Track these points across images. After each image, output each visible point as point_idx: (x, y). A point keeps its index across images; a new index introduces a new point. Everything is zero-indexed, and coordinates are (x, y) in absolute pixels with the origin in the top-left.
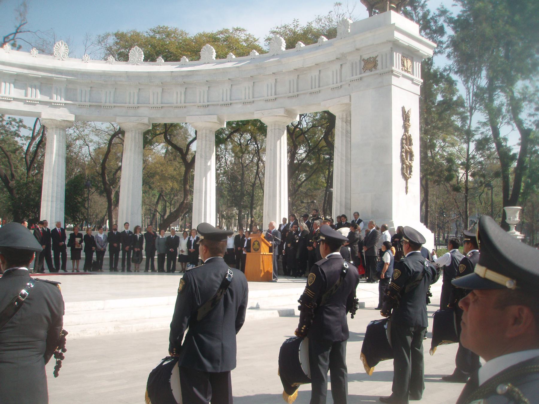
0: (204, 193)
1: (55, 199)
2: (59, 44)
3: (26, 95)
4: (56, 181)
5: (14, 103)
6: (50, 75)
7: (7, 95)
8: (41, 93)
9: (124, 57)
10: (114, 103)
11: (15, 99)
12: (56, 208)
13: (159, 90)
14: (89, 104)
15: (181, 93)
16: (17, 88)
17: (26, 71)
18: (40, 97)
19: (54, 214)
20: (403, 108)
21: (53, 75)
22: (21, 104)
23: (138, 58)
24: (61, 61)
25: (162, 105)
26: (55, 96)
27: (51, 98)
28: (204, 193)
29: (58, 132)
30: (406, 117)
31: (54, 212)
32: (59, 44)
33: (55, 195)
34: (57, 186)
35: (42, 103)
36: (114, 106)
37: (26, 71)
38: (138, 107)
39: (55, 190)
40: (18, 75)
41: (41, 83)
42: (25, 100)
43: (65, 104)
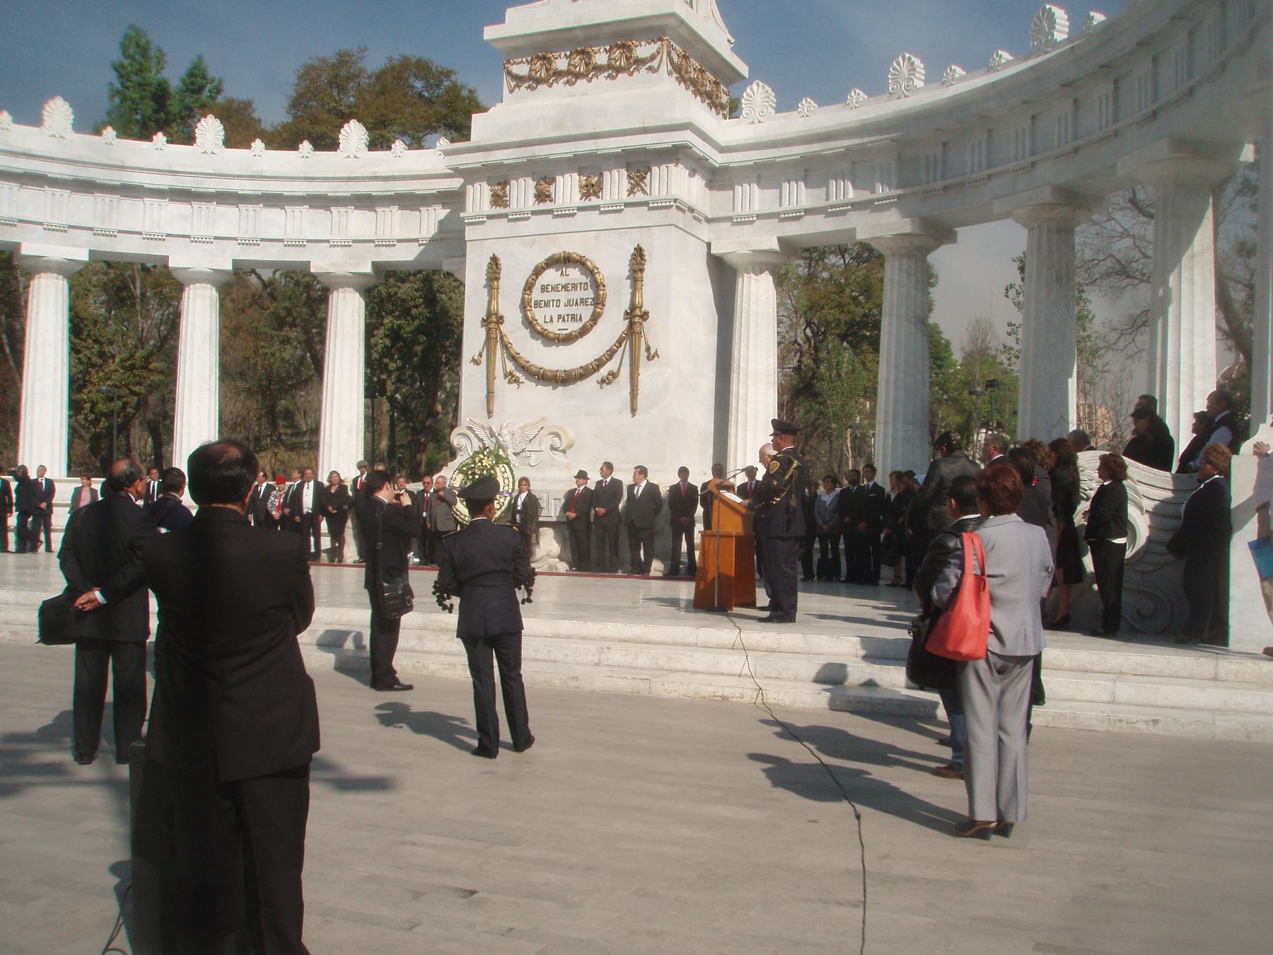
0: (1158, 370)
1: (891, 421)
2: (898, 64)
3: (827, 199)
4: (892, 377)
5: (808, 218)
6: (857, 141)
7: (794, 206)
8: (854, 188)
9: (326, 142)
10: (989, 166)
11: (808, 212)
12: (894, 439)
13: (1068, 105)
14: (940, 184)
15: (1107, 99)
16: (812, 187)
17: (815, 148)
18: (852, 194)
19: (889, 452)
21: (866, 140)
22: (820, 218)
23: (1046, 36)
24: (903, 99)
25: (1075, 144)
26: (879, 188)
27: (873, 192)
28: (1158, 370)
29: (897, 264)
31: (889, 446)
32: (898, 64)
33: (891, 409)
34: (896, 388)
35: (856, 206)
36: (990, 177)
37: (815, 148)
38: (1033, 165)
39: (892, 396)
40: (805, 159)
41: (853, 163)
42: (826, 208)
43: (899, 197)
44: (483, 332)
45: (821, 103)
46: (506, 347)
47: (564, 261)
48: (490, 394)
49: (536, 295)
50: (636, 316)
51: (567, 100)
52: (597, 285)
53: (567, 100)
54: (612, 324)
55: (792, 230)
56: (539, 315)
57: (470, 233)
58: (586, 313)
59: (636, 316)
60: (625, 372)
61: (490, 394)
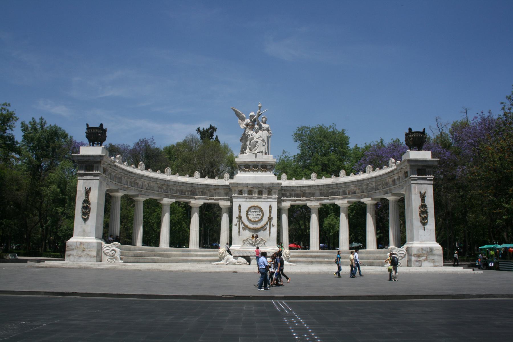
20: (420, 193)
30: (423, 197)
44: (237, 220)
45: (296, 179)
46: (243, 222)
47: (255, 207)
48: (239, 232)
49: (249, 213)
50: (270, 218)
51: (255, 175)
52: (262, 211)
53: (255, 175)
54: (265, 219)
55: (293, 203)
56: (250, 217)
57: (233, 200)
58: (260, 217)
59: (270, 218)
60: (268, 228)
61: (239, 232)
